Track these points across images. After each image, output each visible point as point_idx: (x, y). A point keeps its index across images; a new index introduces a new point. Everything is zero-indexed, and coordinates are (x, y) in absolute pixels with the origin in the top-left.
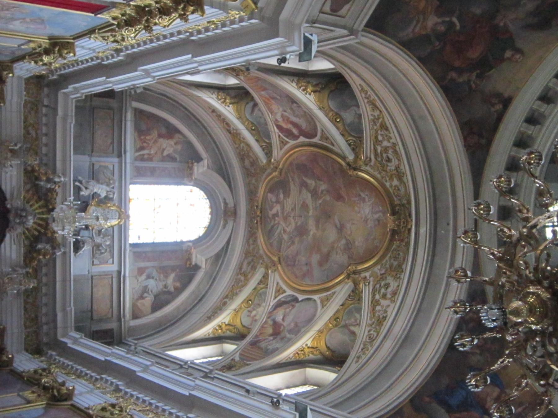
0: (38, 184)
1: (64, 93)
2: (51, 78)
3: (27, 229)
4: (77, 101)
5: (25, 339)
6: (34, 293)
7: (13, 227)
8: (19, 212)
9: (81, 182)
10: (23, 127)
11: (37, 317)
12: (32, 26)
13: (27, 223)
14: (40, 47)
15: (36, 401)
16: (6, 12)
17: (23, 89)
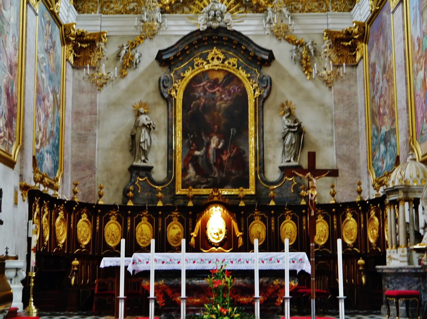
3: (228, 10)
5: (339, 11)
7: (226, 23)
8: (210, 17)
10: (127, 15)
13: (222, 9)
17: (89, 15)
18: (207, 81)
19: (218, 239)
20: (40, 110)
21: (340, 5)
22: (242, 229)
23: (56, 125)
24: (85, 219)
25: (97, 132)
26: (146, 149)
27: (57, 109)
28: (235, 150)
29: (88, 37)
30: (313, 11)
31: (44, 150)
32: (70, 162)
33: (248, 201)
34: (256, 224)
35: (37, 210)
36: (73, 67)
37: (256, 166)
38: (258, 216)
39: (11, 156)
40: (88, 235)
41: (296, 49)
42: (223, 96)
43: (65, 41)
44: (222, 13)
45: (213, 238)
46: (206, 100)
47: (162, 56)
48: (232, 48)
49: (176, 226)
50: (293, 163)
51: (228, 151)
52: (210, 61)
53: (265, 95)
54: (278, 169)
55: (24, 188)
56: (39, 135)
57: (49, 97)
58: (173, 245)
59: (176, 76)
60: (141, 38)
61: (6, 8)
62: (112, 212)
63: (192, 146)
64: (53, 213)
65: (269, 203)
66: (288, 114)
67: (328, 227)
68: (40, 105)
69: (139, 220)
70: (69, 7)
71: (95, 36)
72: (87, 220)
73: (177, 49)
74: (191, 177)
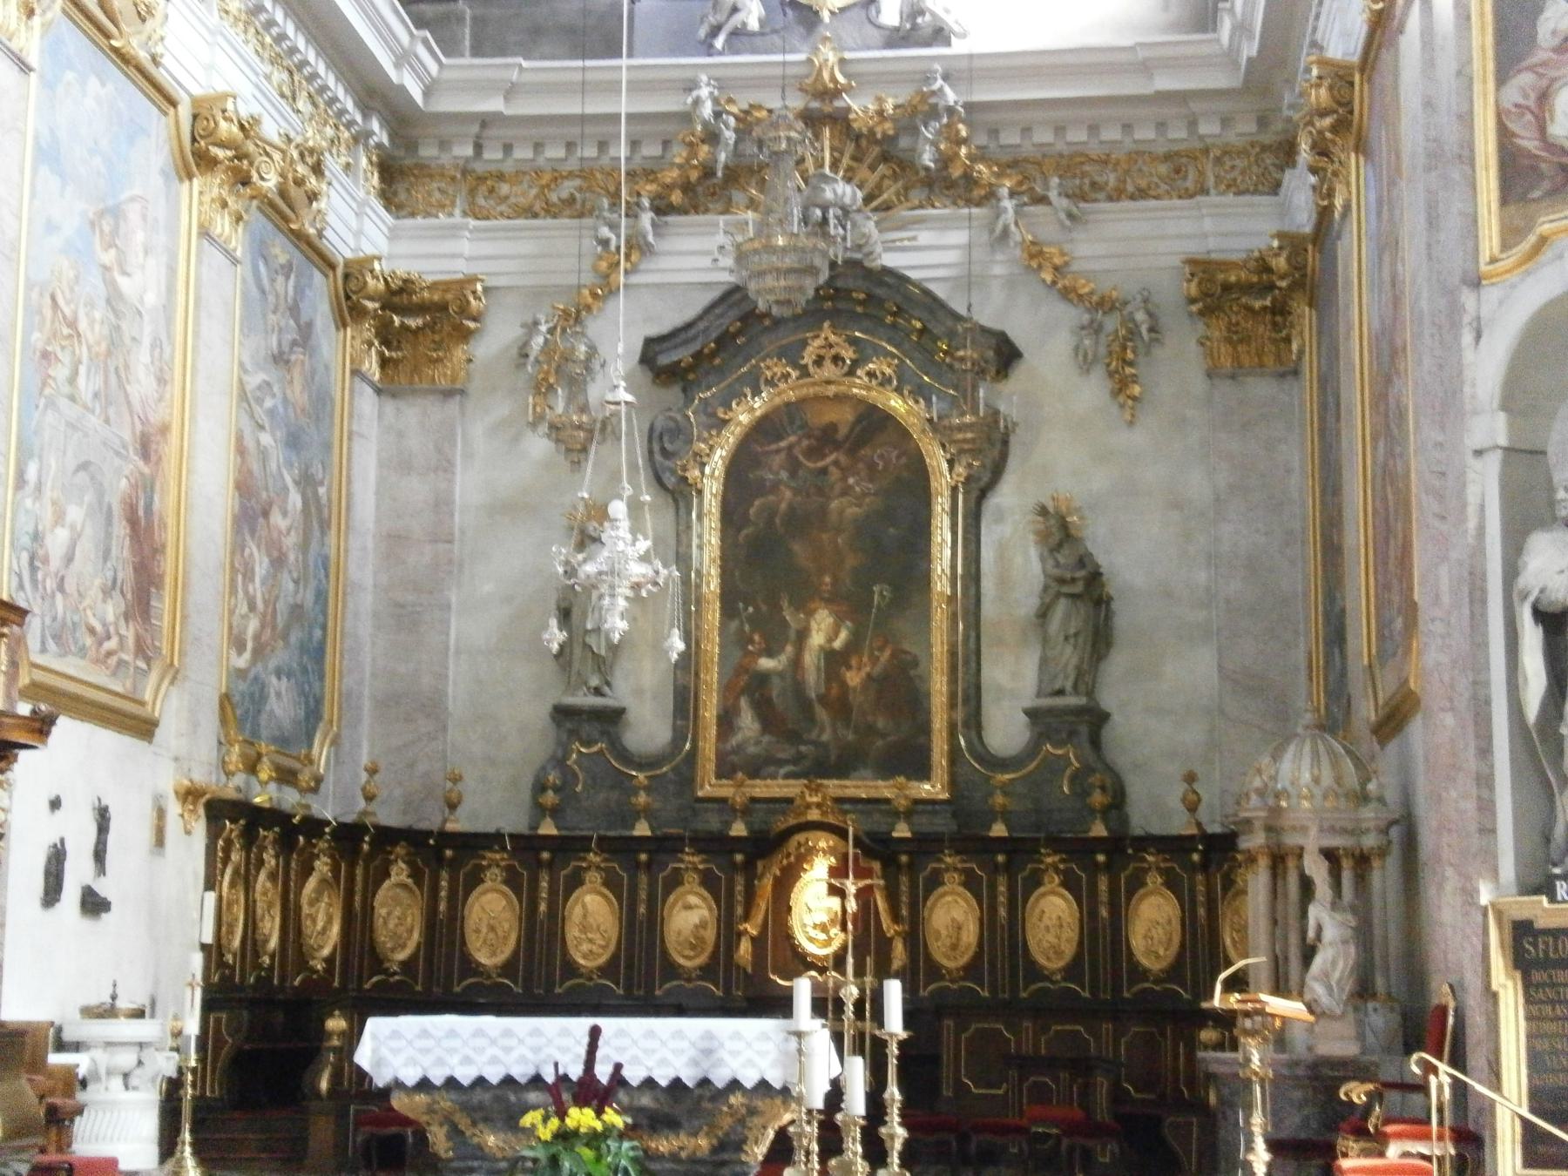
0: (726, 167)
1: (427, 93)
2: (380, 135)
3: (868, 199)
4: (449, 46)
5: (1239, 193)
6: (1087, 168)
7: (859, 247)
9: (715, 31)
10: (549, 221)
11: (1168, 157)
12: (140, 237)
13: (847, 200)
14: (224, 205)
15: (1348, 184)
16: (83, 325)
17: (432, 221)
18: (800, 432)
19: (828, 943)
20: (252, 548)
21: (1243, 173)
22: (904, 912)
23: (313, 584)
24: (404, 878)
25: (454, 599)
26: (603, 653)
27: (317, 533)
28: (887, 654)
29: (426, 294)
30: (1152, 193)
31: (266, 668)
32: (366, 692)
33: (924, 819)
34: (949, 898)
35: (235, 856)
36: (379, 392)
37: (952, 705)
38: (956, 869)
39: (142, 703)
40: (410, 931)
41: (1092, 322)
42: (851, 481)
43: (349, 309)
44: (846, 211)
45: (811, 939)
46: (796, 491)
47: (657, 354)
48: (881, 321)
49: (693, 900)
50: (1072, 701)
51: (865, 659)
52: (811, 369)
53: (986, 479)
54: (1023, 719)
55: (189, 795)
56: (246, 627)
57: (285, 501)
58: (681, 961)
59: (703, 418)
60: (594, 295)
61: (129, 270)
62: (489, 855)
63: (751, 641)
64: (293, 865)
65: (989, 828)
66: (1057, 536)
67: (1178, 912)
68: (253, 532)
69: (575, 882)
70: (363, 204)
71: (446, 291)
72: (410, 881)
73: (707, 329)
74: (746, 741)
